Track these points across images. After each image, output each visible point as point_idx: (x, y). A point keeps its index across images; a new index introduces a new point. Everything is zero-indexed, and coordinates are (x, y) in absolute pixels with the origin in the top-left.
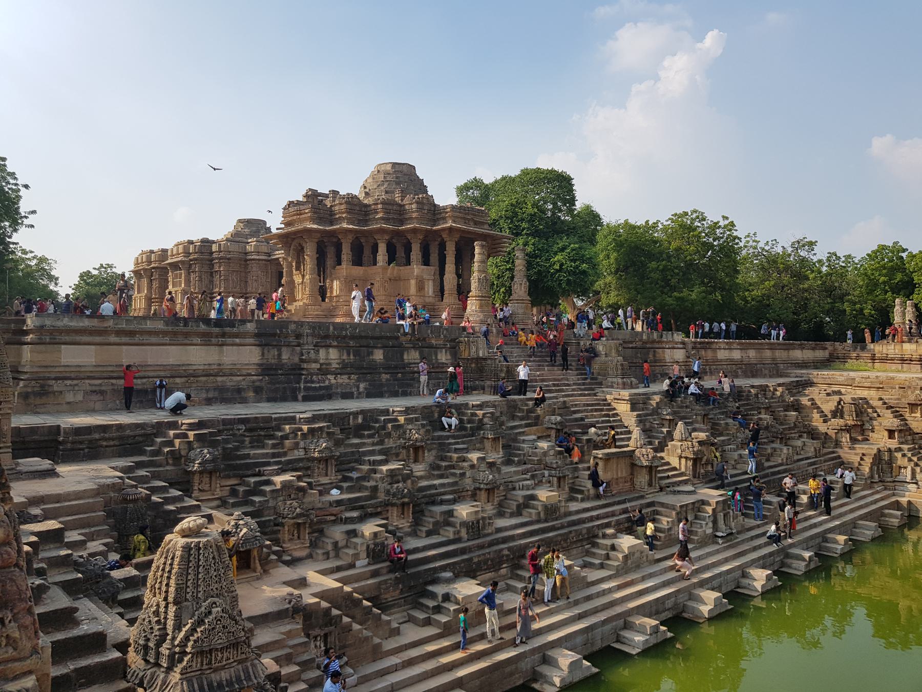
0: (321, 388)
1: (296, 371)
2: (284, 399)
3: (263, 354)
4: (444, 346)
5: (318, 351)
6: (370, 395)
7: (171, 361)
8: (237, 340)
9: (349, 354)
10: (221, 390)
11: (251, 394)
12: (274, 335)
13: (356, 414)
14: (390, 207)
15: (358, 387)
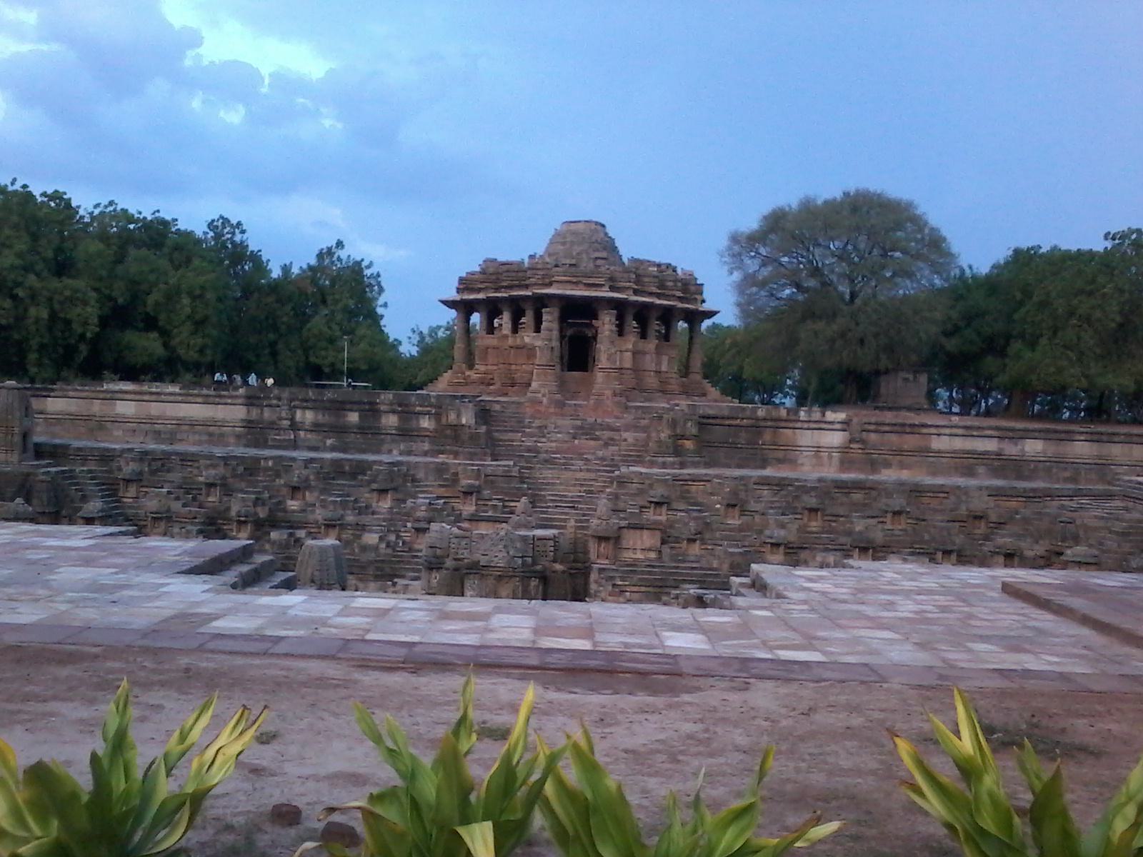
0: (284, 440)
1: (272, 426)
2: (257, 446)
3: (248, 412)
4: (428, 413)
5: (295, 412)
6: (333, 449)
7: (181, 414)
8: (229, 401)
9: (324, 415)
10: (211, 435)
11: (232, 440)
12: (259, 398)
13: (266, 459)
14: (514, 274)
15: (325, 443)
